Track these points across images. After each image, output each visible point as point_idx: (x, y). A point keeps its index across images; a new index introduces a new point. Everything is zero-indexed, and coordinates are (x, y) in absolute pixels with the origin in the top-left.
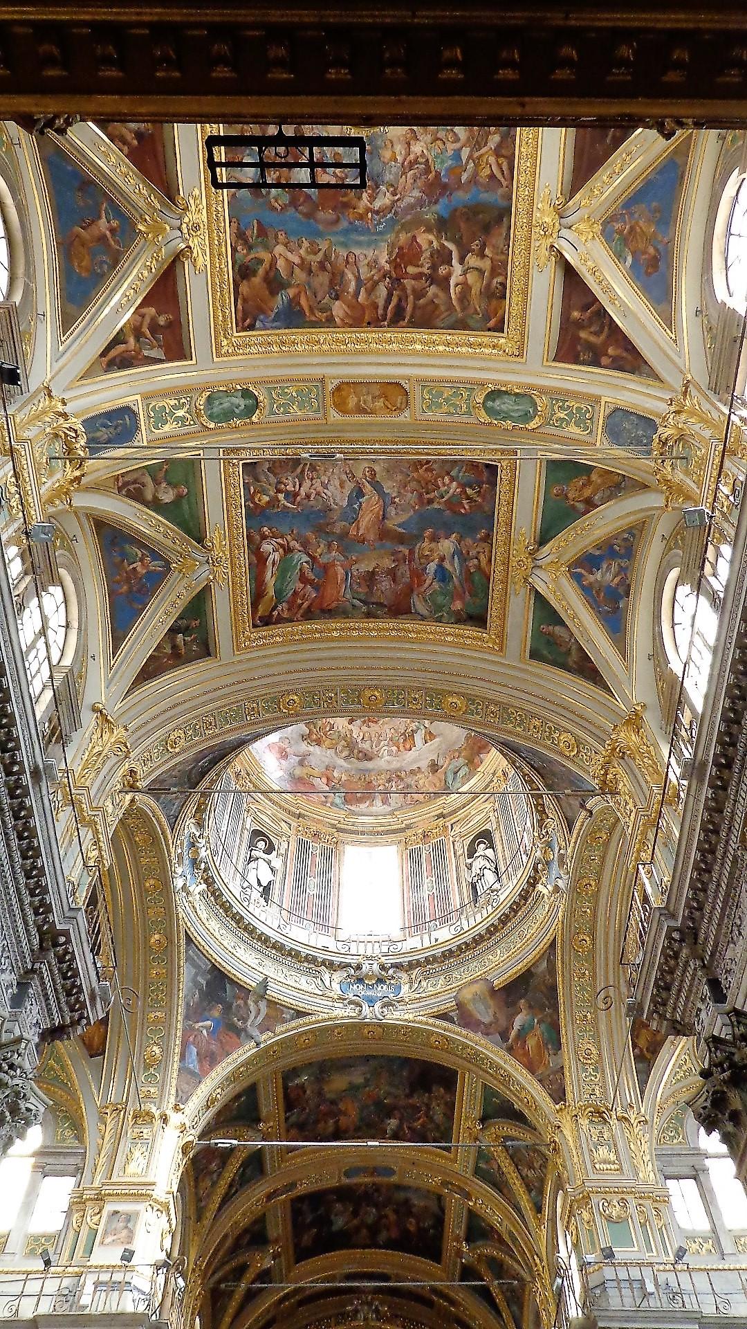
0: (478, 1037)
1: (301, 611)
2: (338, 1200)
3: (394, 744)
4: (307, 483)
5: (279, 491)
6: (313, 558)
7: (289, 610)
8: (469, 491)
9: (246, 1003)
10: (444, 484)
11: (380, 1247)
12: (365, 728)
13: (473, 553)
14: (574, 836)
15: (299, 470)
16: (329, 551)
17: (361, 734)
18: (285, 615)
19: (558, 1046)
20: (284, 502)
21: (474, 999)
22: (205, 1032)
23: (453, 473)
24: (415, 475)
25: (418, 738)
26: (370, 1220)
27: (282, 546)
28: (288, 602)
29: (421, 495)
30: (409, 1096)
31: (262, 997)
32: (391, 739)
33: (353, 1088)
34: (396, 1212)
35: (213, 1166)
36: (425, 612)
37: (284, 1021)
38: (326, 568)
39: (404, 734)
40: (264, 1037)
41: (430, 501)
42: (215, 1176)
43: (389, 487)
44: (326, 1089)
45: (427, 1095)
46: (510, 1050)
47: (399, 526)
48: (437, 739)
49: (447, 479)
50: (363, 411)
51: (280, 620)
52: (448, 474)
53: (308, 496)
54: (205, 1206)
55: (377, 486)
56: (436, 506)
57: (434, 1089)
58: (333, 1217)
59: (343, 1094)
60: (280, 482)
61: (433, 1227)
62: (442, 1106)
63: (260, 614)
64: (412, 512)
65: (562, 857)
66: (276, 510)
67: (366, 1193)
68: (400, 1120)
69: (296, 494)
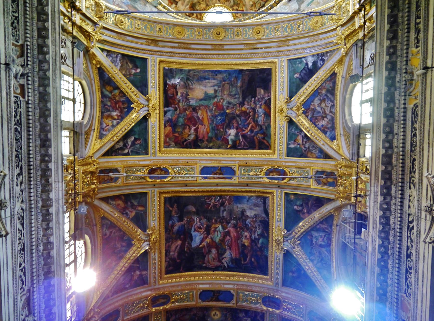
2: (197, 213)
11: (224, 269)
26: (218, 238)
30: (242, 104)
33: (207, 97)
34: (235, 226)
35: (115, 114)
42: (115, 122)
44: (190, 96)
45: (253, 99)
54: (106, 135)
57: (258, 90)
58: (193, 233)
59: (201, 103)
61: (262, 235)
62: (263, 107)
67: (215, 206)
68: (237, 129)
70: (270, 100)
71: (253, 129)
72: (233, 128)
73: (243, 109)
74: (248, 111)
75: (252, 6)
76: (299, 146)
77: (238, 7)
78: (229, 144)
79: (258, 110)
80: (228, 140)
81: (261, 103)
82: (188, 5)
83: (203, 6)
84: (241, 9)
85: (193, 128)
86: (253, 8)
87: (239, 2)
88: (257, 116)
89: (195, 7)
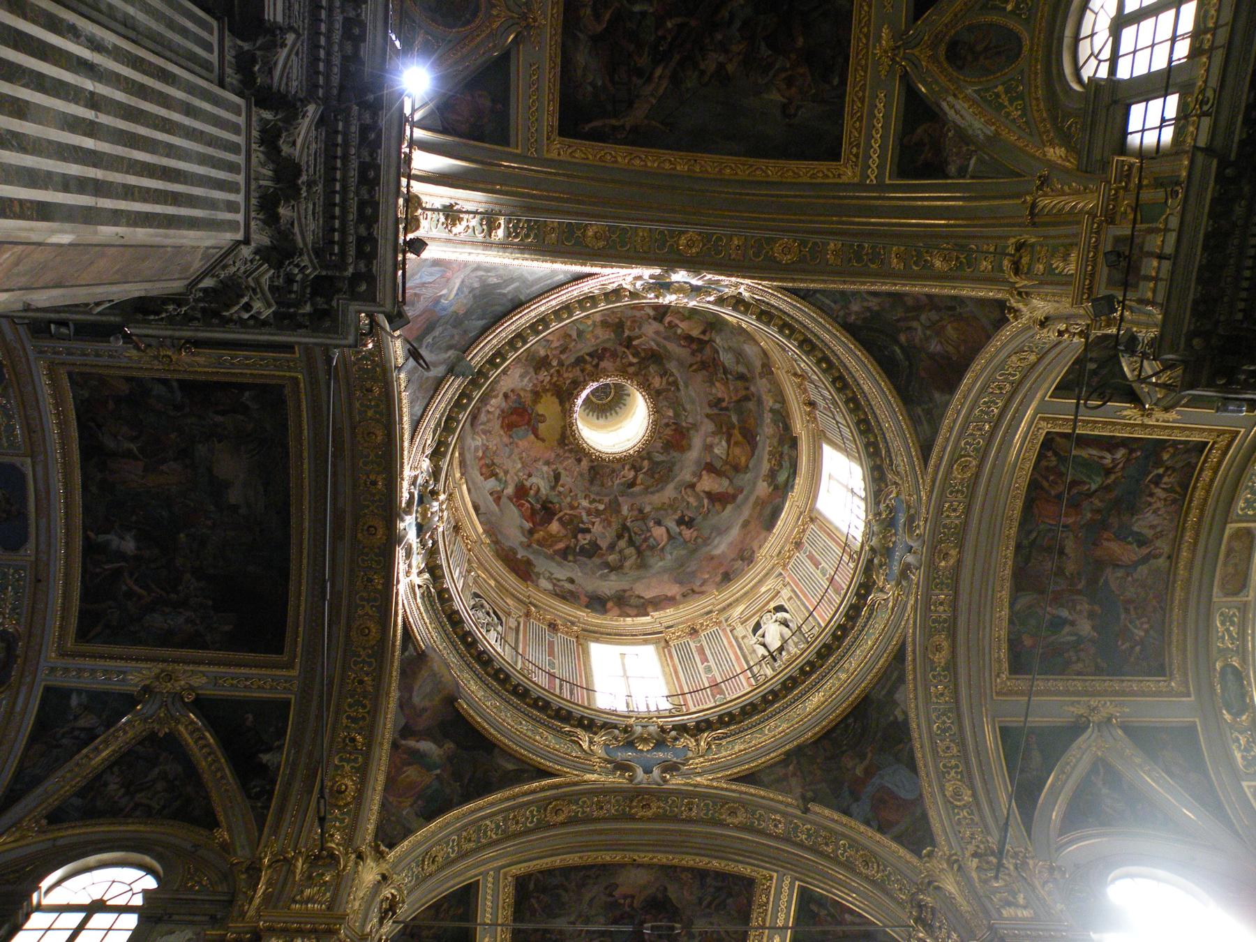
0: (395, 695)
1: (1040, 479)
3: (484, 453)
4: (1162, 494)
5: (1167, 469)
6: (1089, 495)
7: (1047, 468)
8: (1138, 649)
9: (450, 347)
10: (1142, 624)
12: (498, 412)
13: (1082, 655)
14: (734, 787)
15: (1178, 489)
16: (1092, 511)
17: (493, 409)
18: (1044, 463)
19: (429, 817)
20: (1156, 472)
21: (434, 675)
22: (444, 292)
23: (1152, 632)
24: (1151, 596)
25: (492, 483)
27: (1114, 467)
28: (1056, 466)
29: (1129, 602)
31: (451, 370)
32: (487, 448)
36: (1017, 607)
37: (412, 402)
38: (1075, 506)
39: (493, 464)
40: (402, 376)
41: (1127, 611)
43: (1143, 570)
46: (395, 746)
47: (1106, 582)
48: (497, 509)
49: (1146, 626)
50: (1228, 555)
51: (1041, 456)
52: (1152, 627)
53: (1151, 495)
55: (1145, 560)
56: (1123, 617)
60: (1174, 470)
63: (1058, 439)
64: (1117, 592)
65: (671, 768)
66: (1151, 464)
69: (1157, 484)
70: (204, 646)
71: (135, 599)
72: (138, 548)
73: (188, 576)
74: (180, 588)
75: (641, 511)
76: (71, 718)
77: (644, 473)
78: (97, 534)
79: (180, 613)
80: (108, 533)
81: (198, 622)
82: (658, 345)
83: (657, 382)
84: (639, 481)
85: (132, 446)
86: (635, 513)
87: (657, 476)
88: (167, 610)
89: (653, 363)
